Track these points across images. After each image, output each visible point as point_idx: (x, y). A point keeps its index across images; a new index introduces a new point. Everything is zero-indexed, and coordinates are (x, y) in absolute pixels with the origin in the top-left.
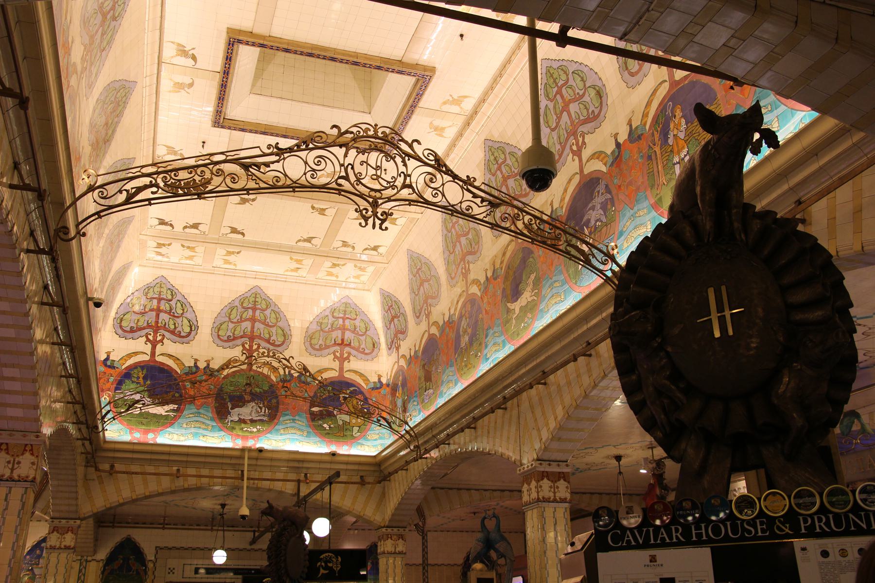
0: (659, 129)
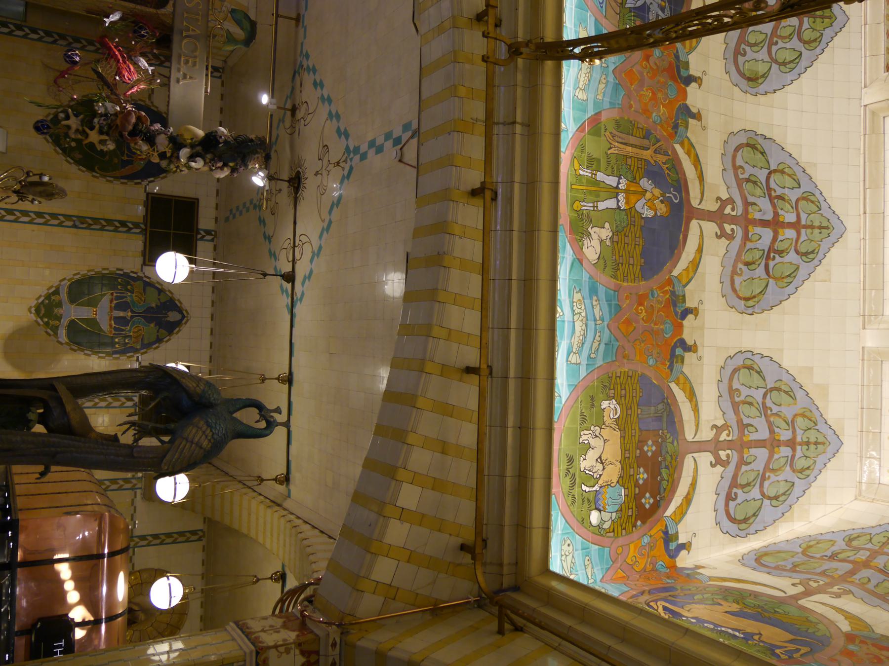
0: (665, 167)
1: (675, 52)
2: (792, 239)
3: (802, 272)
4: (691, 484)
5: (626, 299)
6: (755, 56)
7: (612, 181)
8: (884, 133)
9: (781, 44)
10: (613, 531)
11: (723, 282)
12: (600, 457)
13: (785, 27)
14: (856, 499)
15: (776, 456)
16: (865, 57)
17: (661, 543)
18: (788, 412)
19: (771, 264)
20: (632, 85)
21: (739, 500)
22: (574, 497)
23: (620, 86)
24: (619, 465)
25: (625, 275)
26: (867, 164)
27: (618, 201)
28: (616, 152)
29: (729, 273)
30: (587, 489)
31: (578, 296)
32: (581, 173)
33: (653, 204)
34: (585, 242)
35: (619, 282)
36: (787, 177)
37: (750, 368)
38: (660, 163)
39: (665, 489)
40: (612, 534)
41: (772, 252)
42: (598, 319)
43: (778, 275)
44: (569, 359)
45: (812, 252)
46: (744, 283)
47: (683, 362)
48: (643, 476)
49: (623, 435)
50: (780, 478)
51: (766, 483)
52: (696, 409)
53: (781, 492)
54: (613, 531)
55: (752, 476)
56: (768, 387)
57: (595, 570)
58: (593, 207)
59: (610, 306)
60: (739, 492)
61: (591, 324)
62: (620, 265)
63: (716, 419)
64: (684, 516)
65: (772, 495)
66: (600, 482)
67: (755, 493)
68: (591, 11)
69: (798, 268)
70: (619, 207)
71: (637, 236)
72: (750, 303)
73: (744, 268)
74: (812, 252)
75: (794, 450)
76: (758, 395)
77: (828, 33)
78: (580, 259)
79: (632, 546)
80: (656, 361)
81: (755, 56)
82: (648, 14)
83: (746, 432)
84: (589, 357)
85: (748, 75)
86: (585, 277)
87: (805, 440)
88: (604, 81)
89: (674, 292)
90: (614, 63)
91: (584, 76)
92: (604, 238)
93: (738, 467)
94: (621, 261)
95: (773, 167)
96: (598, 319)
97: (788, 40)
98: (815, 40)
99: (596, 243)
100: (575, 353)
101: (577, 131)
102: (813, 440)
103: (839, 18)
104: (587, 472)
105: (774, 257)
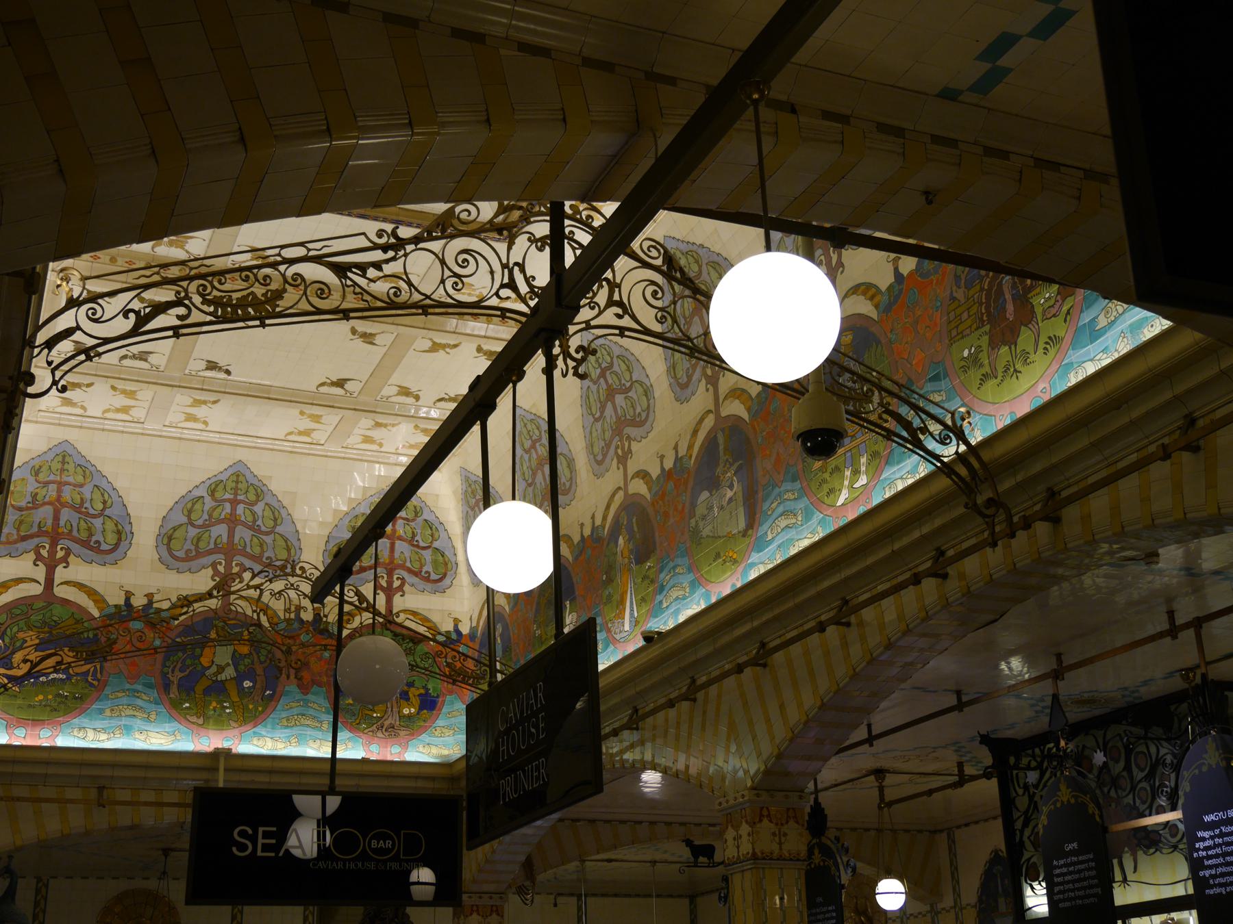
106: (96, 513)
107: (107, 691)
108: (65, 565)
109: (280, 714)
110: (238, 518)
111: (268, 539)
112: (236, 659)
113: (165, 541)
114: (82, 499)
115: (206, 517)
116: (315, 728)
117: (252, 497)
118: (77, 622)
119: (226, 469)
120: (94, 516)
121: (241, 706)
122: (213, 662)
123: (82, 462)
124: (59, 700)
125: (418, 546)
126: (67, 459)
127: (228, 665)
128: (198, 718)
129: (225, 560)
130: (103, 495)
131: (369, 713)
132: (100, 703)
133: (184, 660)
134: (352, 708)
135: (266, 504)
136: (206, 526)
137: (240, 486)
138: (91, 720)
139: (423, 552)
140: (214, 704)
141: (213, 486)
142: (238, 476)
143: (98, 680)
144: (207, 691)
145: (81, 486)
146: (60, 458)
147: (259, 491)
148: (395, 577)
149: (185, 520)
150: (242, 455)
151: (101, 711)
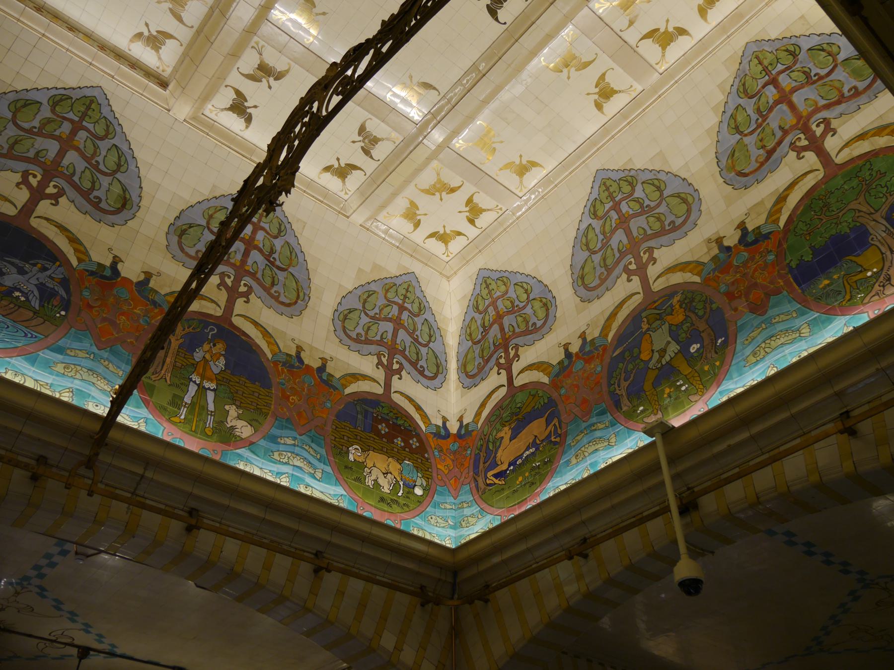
0: (187, 330)
1: (87, 273)
2: (265, 236)
3: (292, 241)
4: (410, 401)
5: (283, 410)
6: (103, 189)
7: (193, 389)
8: (215, 121)
9: (100, 159)
10: (428, 478)
11: (282, 313)
12: (384, 474)
13: (85, 147)
14: (449, 281)
15: (406, 324)
16: (142, 95)
17: (441, 442)
18: (381, 302)
19: (278, 263)
20: (113, 334)
21: (425, 366)
22: (404, 504)
23: (113, 347)
24: (390, 459)
25: (265, 404)
26: (231, 146)
27: (209, 389)
28: (169, 375)
29: (276, 304)
30: (401, 492)
31: (276, 456)
32: (183, 417)
33: (215, 354)
34: (238, 434)
35: (270, 412)
36: (215, 215)
37: (345, 317)
38: (183, 333)
39: (410, 426)
40: (430, 480)
41: (269, 256)
42: (294, 442)
43: (287, 262)
44: (319, 478)
45: (280, 225)
46: (286, 294)
47: (333, 376)
48: (399, 441)
49: (372, 449)
50: (420, 329)
51: (420, 340)
52: (365, 377)
53: (428, 330)
54: (428, 478)
55: (413, 349)
56: (361, 308)
57: (448, 501)
58: (211, 415)
59: (287, 428)
60: (421, 363)
61: (297, 450)
62: (258, 406)
63: (372, 362)
64: (427, 416)
65: (428, 339)
66: (399, 479)
67: (424, 350)
68: (39, 351)
69: (288, 243)
70: (214, 390)
71: (238, 381)
72: (301, 295)
73: (275, 288)
74: (280, 225)
75: (406, 309)
76: (365, 320)
77: (105, 111)
78: (249, 444)
79: (439, 466)
80: (329, 400)
81: (103, 189)
82: (48, 287)
83: (385, 340)
84: (319, 460)
85: (119, 206)
86: (263, 443)
87: (402, 297)
88: (107, 363)
89: (283, 362)
90: (91, 345)
91: (99, 382)
92: (236, 414)
93: (406, 358)
94: (255, 405)
95: (204, 224)
96: (294, 442)
97: (98, 150)
98: (108, 126)
99: (240, 424)
100: (315, 472)
101: (147, 408)
102: (404, 292)
103: (96, 94)
104: (391, 488)
105: (273, 258)
106: (524, 303)
107: (569, 441)
108: (517, 359)
109: (743, 354)
110: (626, 216)
111: (662, 209)
112: (674, 334)
113: (580, 283)
114: (511, 302)
115: (601, 237)
116: (793, 341)
117: (627, 189)
118: (534, 396)
119: (592, 188)
120: (524, 307)
121: (696, 374)
122: (653, 351)
123: (498, 275)
124: (533, 473)
125: (821, 78)
126: (489, 281)
127: (668, 343)
128: (656, 414)
129: (633, 257)
130: (522, 287)
131: (860, 276)
132: (566, 455)
133: (626, 367)
134: (831, 287)
135: (643, 183)
136: (605, 245)
137: (611, 190)
138: (561, 476)
139: (833, 77)
140: (667, 390)
141: (592, 209)
142: (604, 184)
143: (560, 436)
144: (657, 383)
145: (507, 292)
146: (484, 285)
147: (629, 179)
148: (814, 127)
149: (587, 253)
150: (595, 164)
151: (568, 462)
